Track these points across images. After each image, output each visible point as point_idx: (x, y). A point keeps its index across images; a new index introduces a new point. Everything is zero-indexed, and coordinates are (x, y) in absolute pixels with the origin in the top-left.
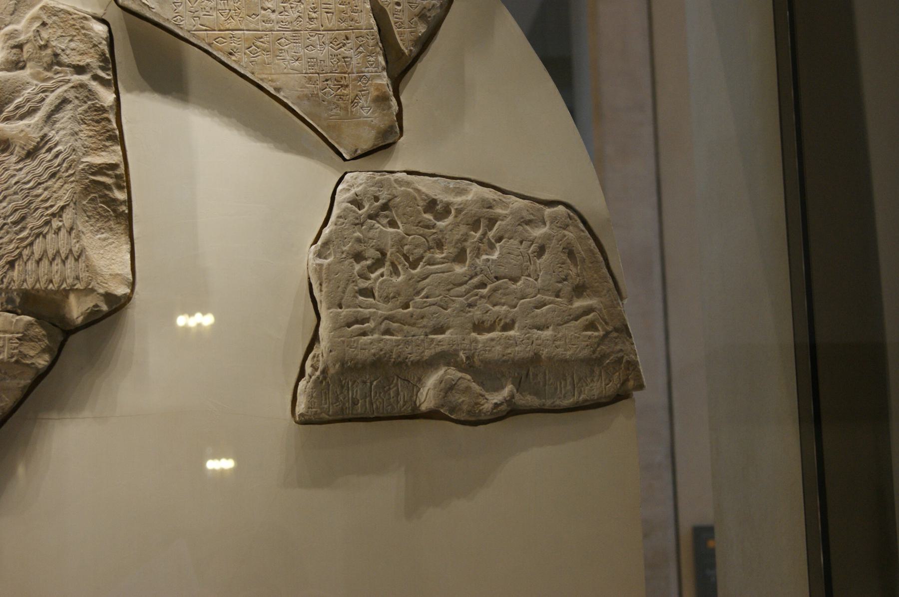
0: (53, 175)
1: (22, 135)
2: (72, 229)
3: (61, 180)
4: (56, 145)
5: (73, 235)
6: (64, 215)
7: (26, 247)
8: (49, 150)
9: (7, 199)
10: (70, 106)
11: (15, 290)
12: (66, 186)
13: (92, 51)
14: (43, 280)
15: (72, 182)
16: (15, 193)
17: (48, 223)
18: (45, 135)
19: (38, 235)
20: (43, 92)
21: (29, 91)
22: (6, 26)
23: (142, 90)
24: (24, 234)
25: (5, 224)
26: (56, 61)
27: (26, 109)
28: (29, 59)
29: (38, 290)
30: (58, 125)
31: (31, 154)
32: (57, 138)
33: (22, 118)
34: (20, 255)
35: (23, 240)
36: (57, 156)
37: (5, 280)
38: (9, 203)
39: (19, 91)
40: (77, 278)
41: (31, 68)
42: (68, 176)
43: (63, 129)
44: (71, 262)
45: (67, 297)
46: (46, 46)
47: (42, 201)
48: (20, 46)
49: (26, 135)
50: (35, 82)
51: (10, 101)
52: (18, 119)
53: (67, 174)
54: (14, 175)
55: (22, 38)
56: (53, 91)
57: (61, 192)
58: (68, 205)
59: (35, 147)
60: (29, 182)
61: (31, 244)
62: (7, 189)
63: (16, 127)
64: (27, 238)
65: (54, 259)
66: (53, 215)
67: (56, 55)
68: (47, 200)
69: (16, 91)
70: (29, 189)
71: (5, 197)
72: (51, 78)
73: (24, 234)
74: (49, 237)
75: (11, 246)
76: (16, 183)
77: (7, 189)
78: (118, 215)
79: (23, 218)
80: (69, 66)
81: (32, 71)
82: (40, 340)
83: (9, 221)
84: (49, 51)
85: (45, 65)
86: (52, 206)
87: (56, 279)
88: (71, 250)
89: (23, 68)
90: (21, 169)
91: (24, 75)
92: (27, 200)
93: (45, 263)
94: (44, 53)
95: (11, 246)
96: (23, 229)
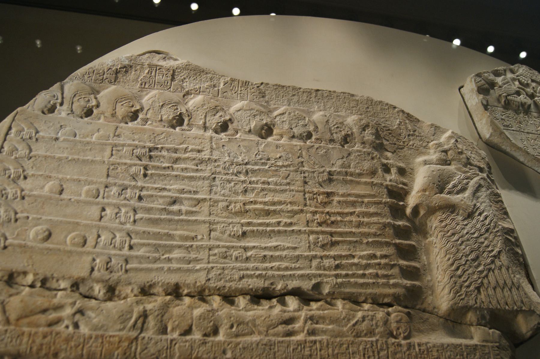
0: (487, 230)
1: (463, 203)
2: (509, 267)
3: (492, 234)
4: (483, 212)
5: (510, 271)
6: (501, 257)
7: (484, 278)
8: (480, 214)
9: (464, 243)
10: (484, 189)
11: (486, 309)
12: (496, 238)
13: (482, 161)
14: (502, 302)
15: (499, 236)
16: (468, 240)
17: (493, 262)
18: (475, 205)
19: (489, 270)
20: (466, 179)
21: (458, 177)
22: (432, 141)
23: (510, 189)
24: (480, 269)
25: (467, 260)
26: (468, 163)
27: (459, 187)
28: (453, 160)
29: (499, 310)
30: (480, 200)
31: (470, 216)
32: (482, 208)
33: (458, 193)
34: (482, 283)
35: (481, 272)
36: (486, 218)
37: (478, 301)
38: (466, 247)
39: (452, 177)
40: (522, 302)
41: (455, 165)
42: (496, 232)
43: (484, 202)
44: (514, 290)
45: (516, 316)
46: (461, 153)
47: (486, 246)
48: (446, 152)
49: (465, 203)
50: (460, 173)
51: (448, 183)
52: (455, 194)
53: (495, 230)
54: (464, 228)
55: (446, 147)
56: (472, 179)
57: (495, 242)
58: (502, 250)
59: (472, 211)
60: (474, 233)
61: (487, 276)
62: (462, 237)
63: (458, 198)
64: (483, 271)
65: (504, 288)
66: (495, 256)
67: (468, 159)
68: (488, 246)
69: (451, 177)
70: (476, 238)
71: (462, 242)
72: (468, 172)
73: (480, 269)
74: (496, 272)
75: (475, 276)
76: (467, 233)
77: (462, 237)
78: (520, 264)
79: (477, 257)
80: (476, 166)
81: (456, 166)
82: (508, 350)
83: (469, 258)
84: (464, 156)
85: (463, 163)
86: (492, 251)
87: (509, 301)
88: (513, 283)
89: (449, 164)
90: (466, 225)
91: (452, 168)
92: (477, 245)
93: (498, 290)
94: (461, 157)
95: (475, 276)
96: (479, 265)
